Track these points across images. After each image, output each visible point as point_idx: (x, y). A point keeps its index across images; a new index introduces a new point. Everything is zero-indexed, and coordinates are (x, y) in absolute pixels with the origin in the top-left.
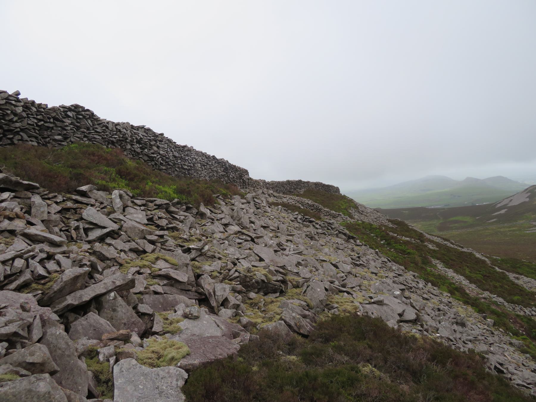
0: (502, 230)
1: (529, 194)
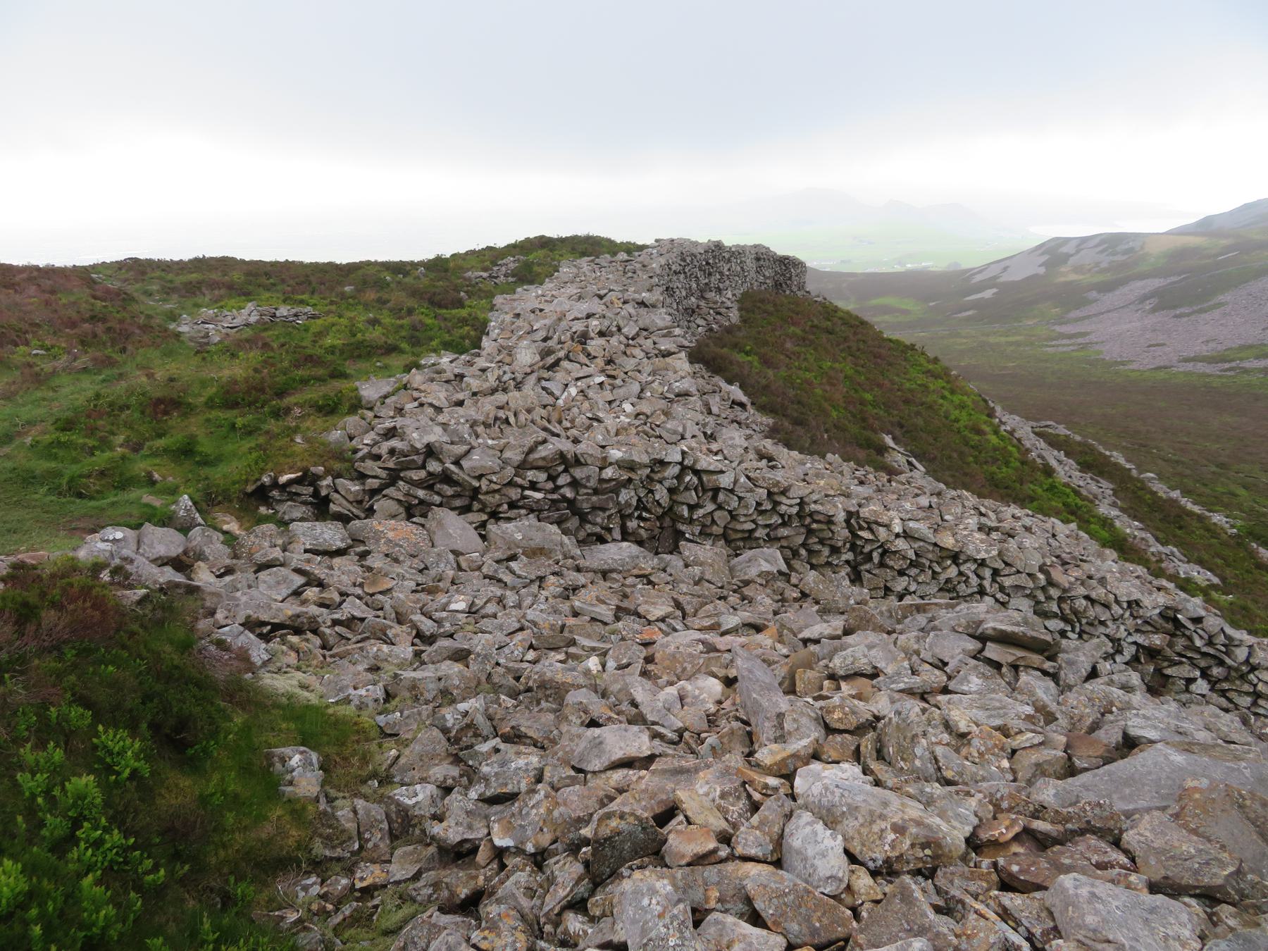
0: (992, 340)
1: (1046, 257)
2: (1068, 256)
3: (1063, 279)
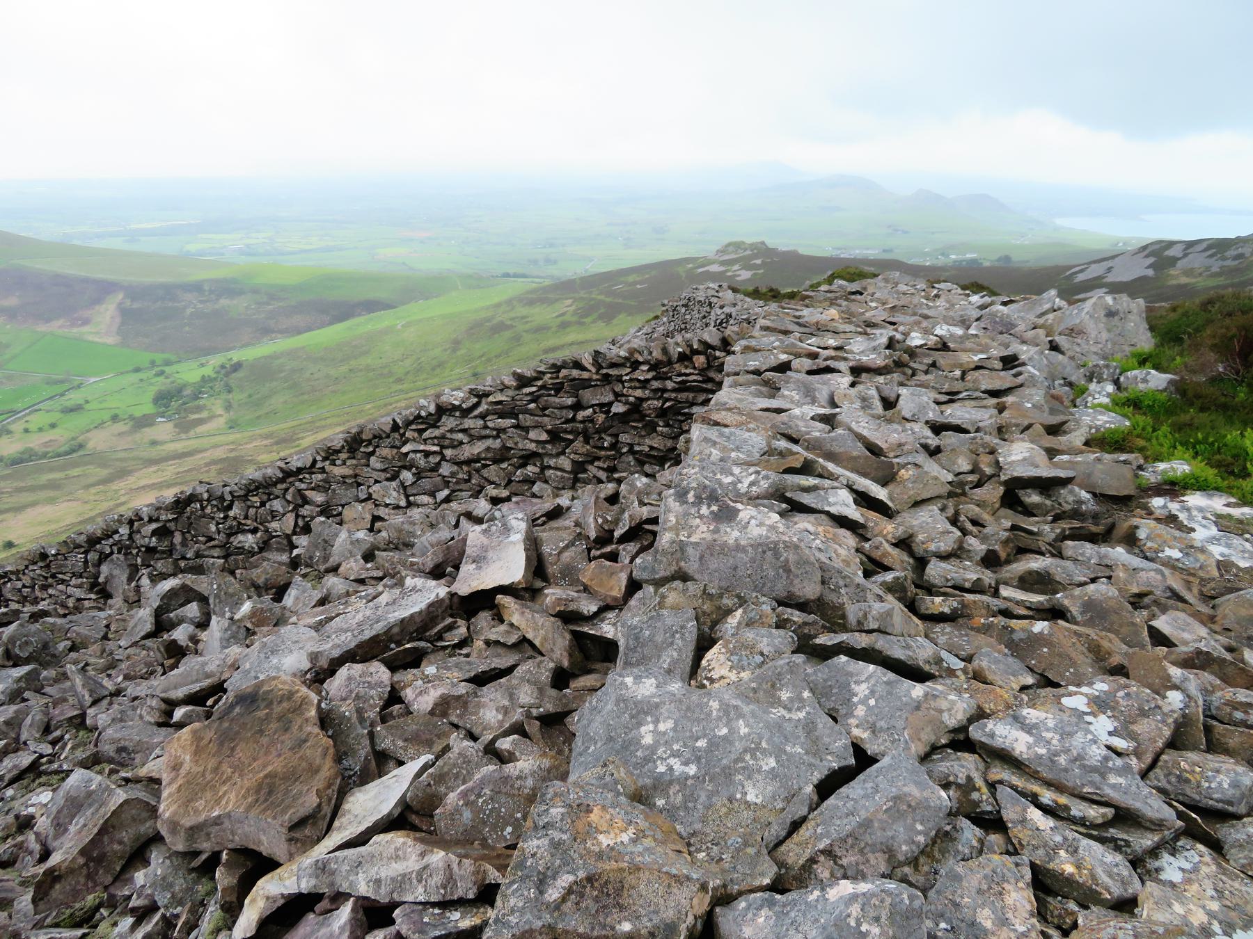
1: (1151, 260)
2: (1173, 261)
3: (1174, 282)
